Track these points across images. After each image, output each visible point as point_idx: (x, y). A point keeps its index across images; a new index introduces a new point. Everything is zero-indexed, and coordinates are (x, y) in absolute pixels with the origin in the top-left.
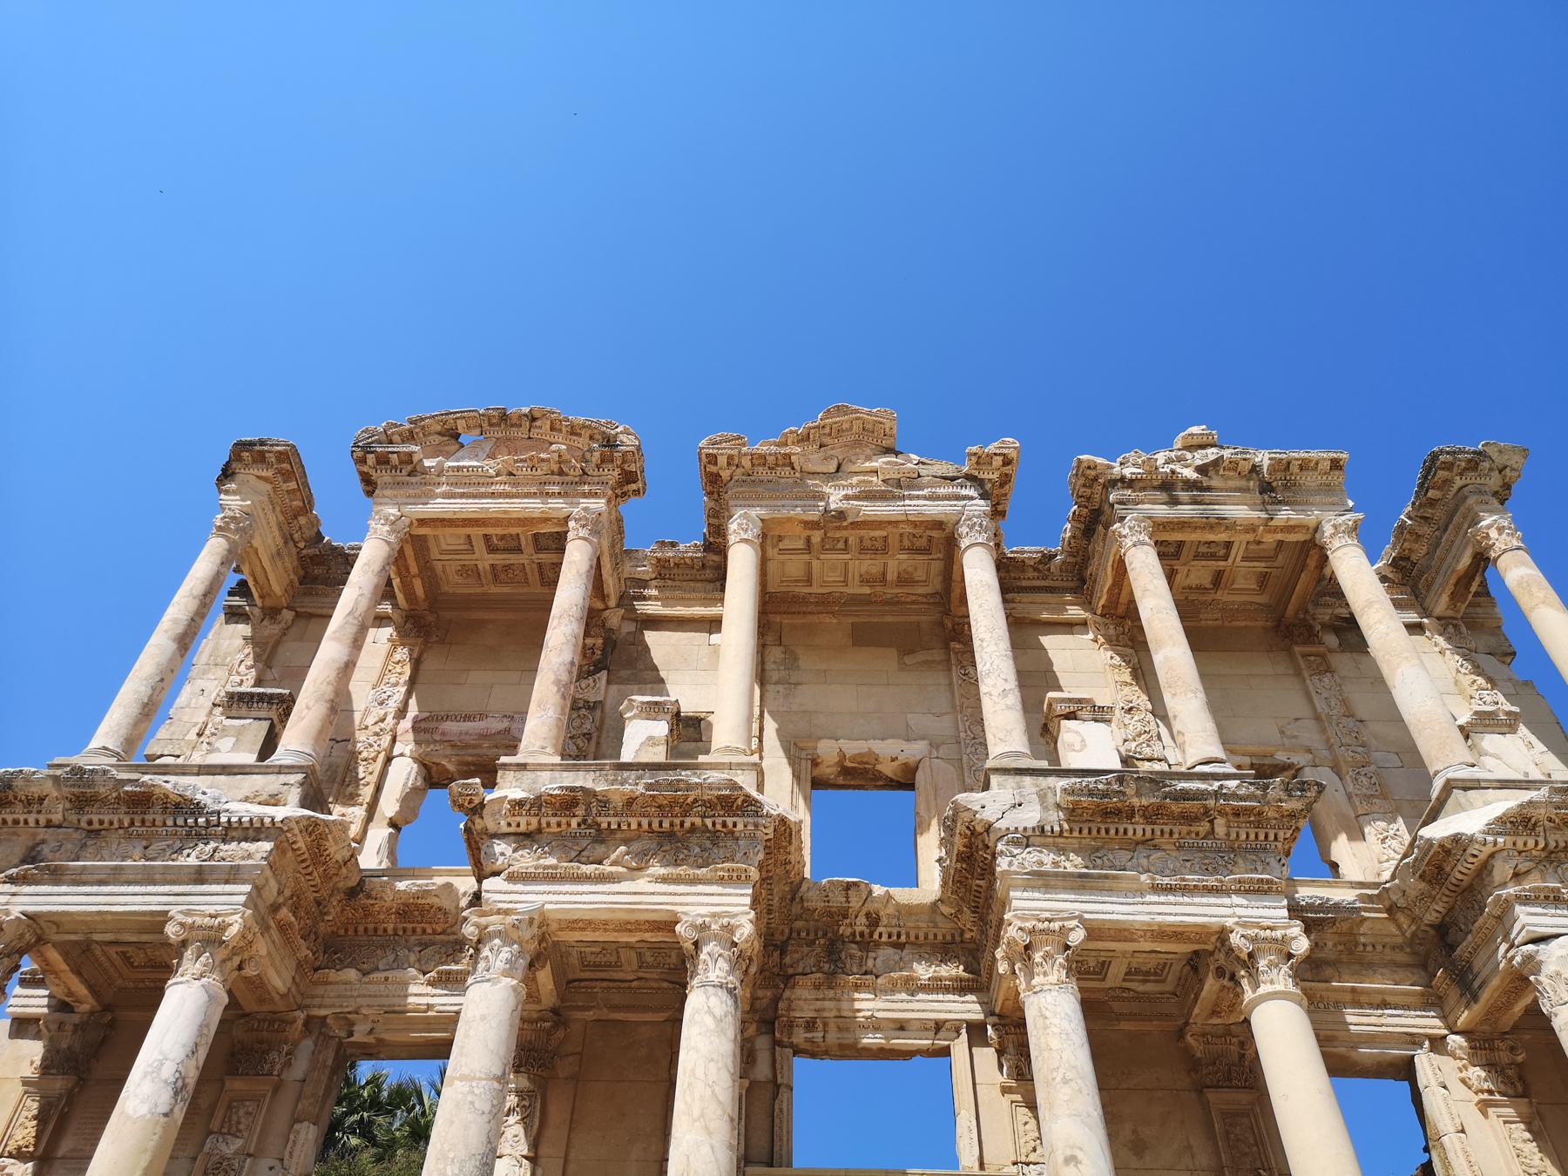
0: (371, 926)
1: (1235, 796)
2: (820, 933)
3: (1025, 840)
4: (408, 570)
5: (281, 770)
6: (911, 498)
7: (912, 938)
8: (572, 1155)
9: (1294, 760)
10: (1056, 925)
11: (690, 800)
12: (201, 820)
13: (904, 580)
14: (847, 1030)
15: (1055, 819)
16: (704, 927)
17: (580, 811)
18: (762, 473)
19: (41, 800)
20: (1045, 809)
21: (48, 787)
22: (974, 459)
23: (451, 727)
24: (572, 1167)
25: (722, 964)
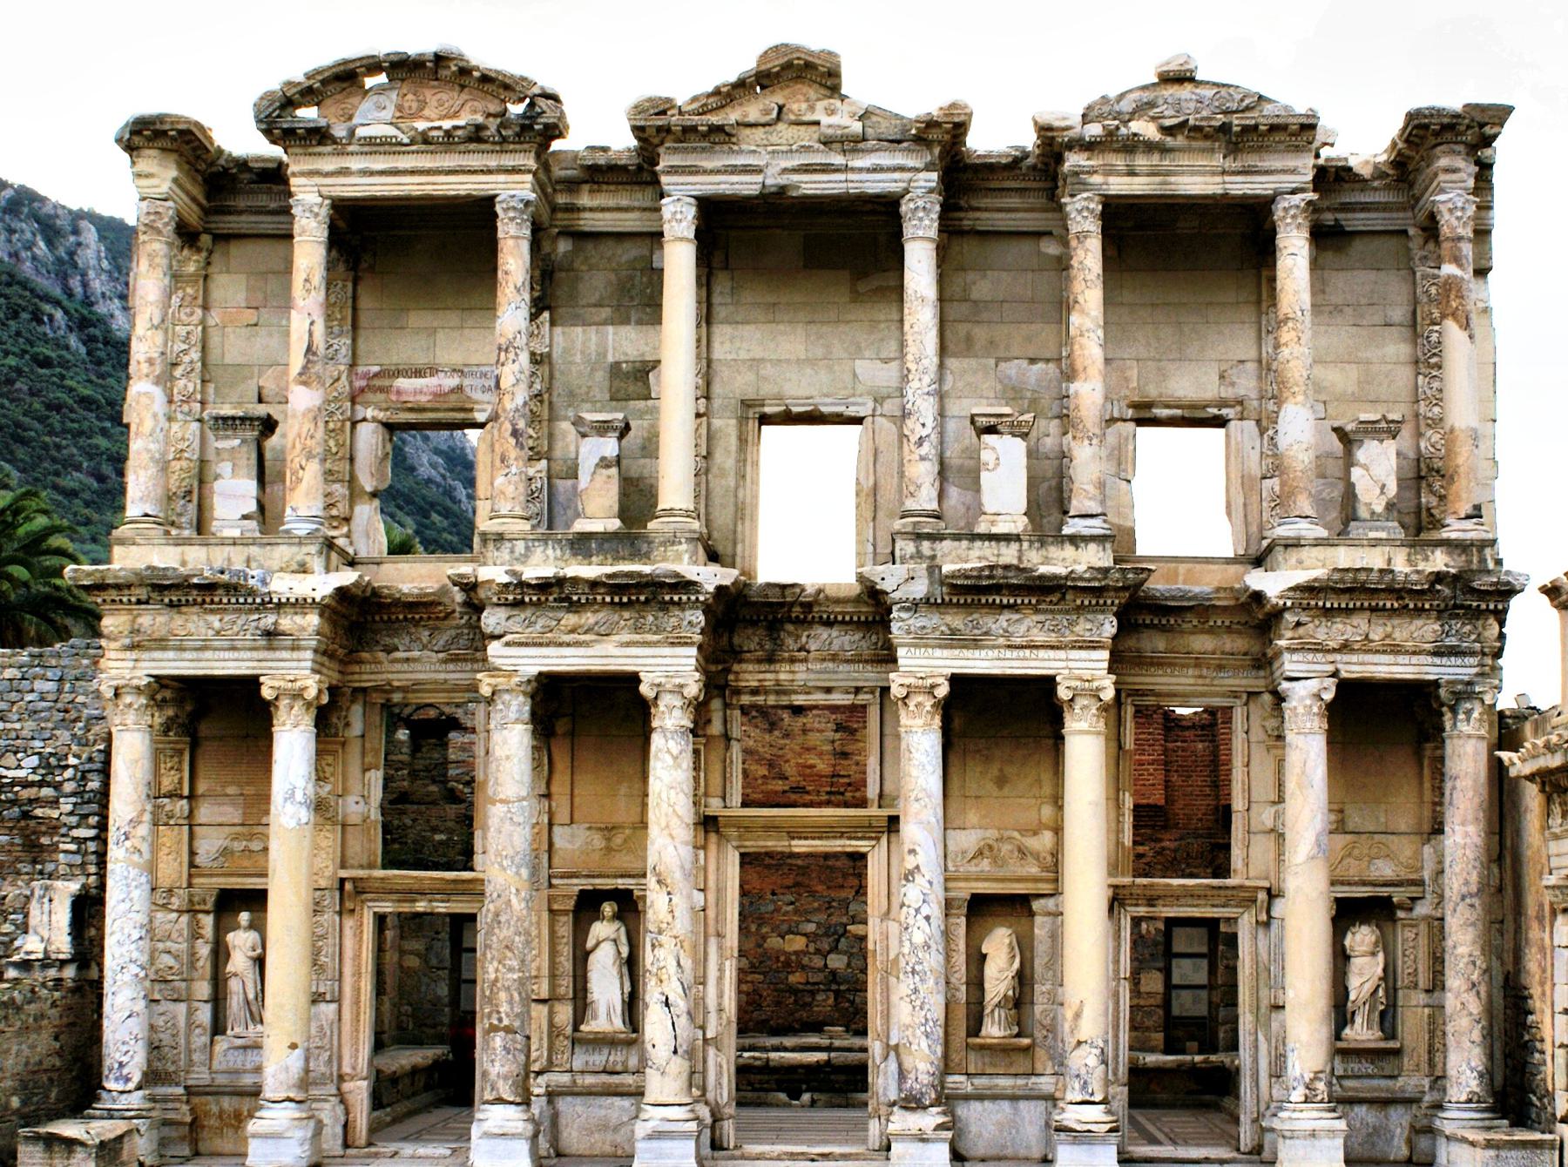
1: (1081, 579)
3: (914, 606)
5: (300, 541)
6: (853, 170)
8: (576, 792)
9: (1224, 411)
10: (929, 682)
12: (258, 600)
14: (785, 692)
15: (939, 593)
16: (659, 685)
17: (556, 590)
20: (931, 583)
23: (402, 383)
24: (577, 800)
25: (677, 713)
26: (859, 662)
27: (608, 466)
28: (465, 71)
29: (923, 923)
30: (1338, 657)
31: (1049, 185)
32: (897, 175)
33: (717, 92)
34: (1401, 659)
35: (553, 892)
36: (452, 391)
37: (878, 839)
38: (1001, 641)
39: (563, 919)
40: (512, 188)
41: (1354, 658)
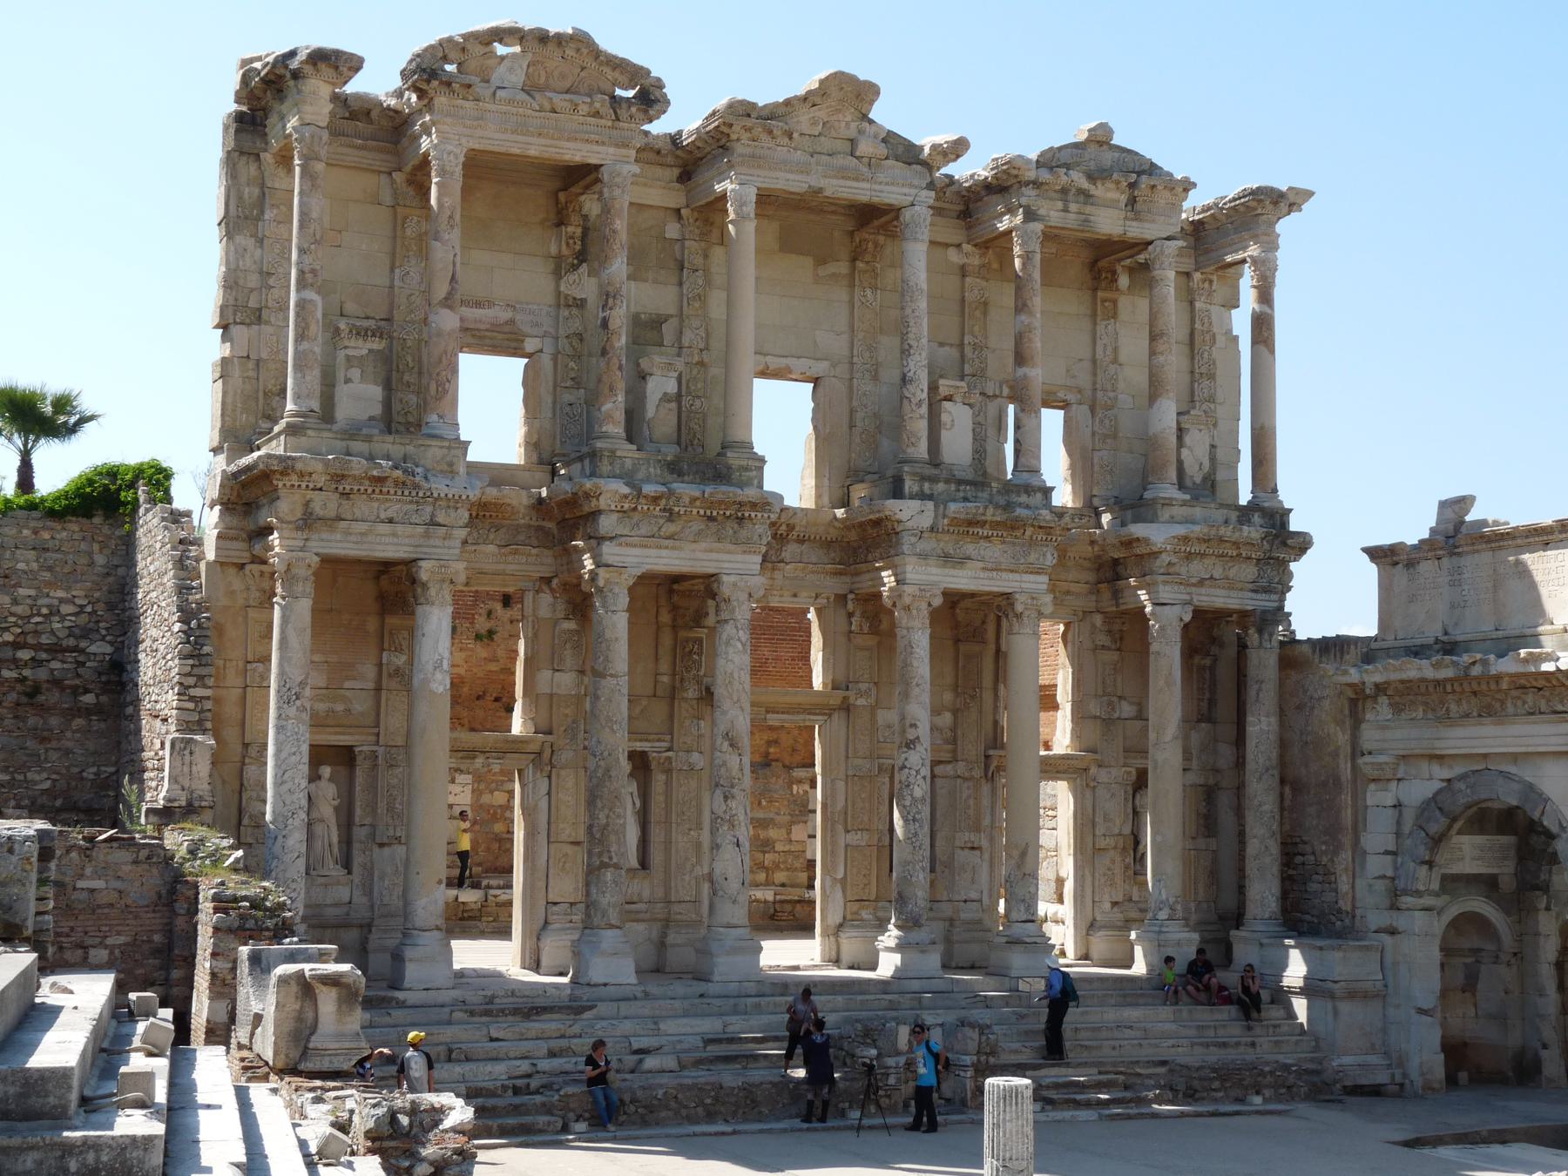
9: (1071, 397)
16: (735, 585)
17: (663, 502)
19: (310, 474)
20: (936, 517)
21: (319, 467)
27: (669, 401)
28: (596, 53)
29: (921, 781)
30: (1194, 589)
31: (961, 207)
32: (906, 190)
33: (788, 102)
34: (1233, 594)
36: (506, 323)
37: (830, 715)
38: (981, 565)
40: (618, 163)
41: (1203, 591)
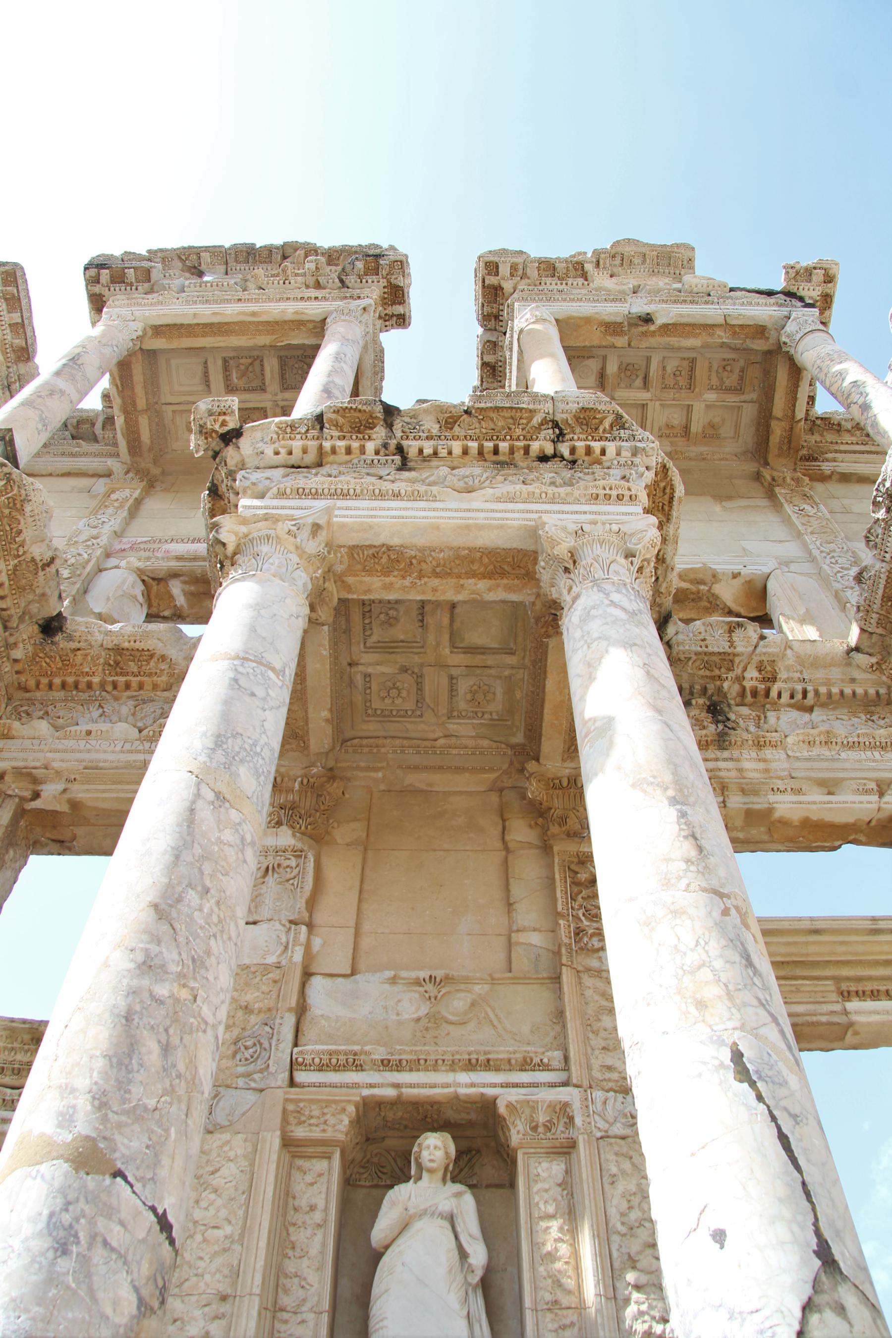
0: (70, 680)
2: (697, 687)
4: (134, 404)
7: (823, 698)
8: (366, 927)
11: (537, 420)
13: (711, 433)
14: (755, 793)
17: (380, 432)
18: (552, 284)
22: (792, 273)
24: (366, 942)
26: (872, 747)
35: (294, 1093)
39: (321, 1165)
